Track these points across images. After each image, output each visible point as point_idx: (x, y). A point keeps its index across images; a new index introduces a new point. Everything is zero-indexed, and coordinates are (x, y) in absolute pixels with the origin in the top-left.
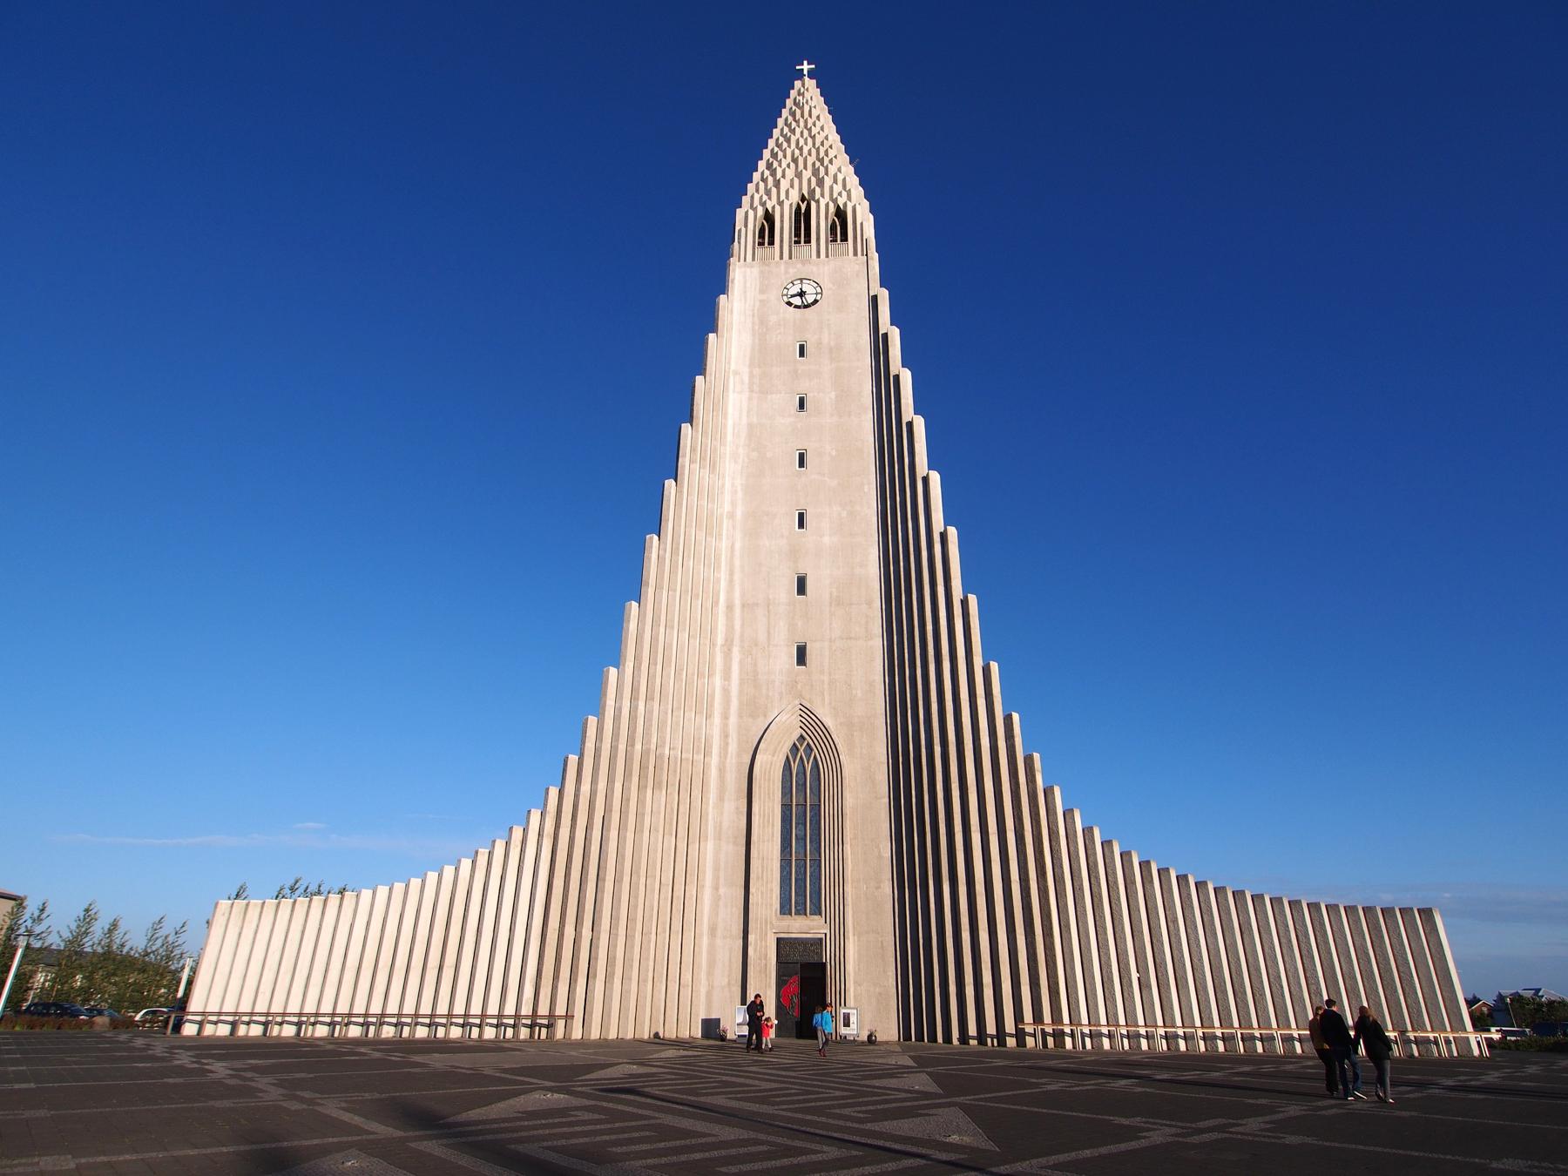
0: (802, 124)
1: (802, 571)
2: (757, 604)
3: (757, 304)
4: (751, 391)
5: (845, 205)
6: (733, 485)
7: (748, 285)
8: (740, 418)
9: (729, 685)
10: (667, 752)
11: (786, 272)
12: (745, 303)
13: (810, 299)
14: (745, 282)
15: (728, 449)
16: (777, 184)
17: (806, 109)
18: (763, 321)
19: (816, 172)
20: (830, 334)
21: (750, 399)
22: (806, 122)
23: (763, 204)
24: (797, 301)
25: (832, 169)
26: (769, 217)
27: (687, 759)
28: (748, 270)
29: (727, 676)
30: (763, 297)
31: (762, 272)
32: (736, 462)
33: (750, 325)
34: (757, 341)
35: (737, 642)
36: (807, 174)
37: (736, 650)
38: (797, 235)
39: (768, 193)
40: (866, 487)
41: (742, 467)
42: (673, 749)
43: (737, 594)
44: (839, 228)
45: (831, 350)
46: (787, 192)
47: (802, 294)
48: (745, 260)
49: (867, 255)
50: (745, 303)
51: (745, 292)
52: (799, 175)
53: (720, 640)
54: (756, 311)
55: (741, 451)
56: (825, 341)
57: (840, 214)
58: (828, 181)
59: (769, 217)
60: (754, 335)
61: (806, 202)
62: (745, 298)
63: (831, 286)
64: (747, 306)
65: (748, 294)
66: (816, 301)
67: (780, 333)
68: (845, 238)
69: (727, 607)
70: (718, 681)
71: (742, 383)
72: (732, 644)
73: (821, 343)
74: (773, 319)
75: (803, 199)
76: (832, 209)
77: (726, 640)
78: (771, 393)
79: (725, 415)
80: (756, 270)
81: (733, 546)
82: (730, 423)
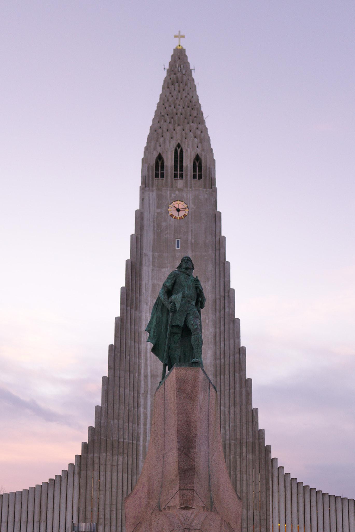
0: (177, 88)
2: (158, 375)
3: (156, 214)
4: (154, 266)
5: (202, 154)
6: (146, 316)
7: (151, 202)
8: (148, 281)
9: (146, 411)
10: (123, 441)
11: (171, 196)
12: (150, 214)
13: (182, 214)
14: (149, 201)
15: (143, 298)
18: (159, 226)
20: (192, 235)
21: (153, 270)
22: (179, 86)
24: (175, 213)
26: (160, 158)
27: (130, 443)
28: (151, 193)
29: (145, 408)
30: (159, 211)
31: (158, 195)
32: (147, 304)
33: (152, 227)
34: (156, 236)
35: (149, 392)
37: (149, 396)
38: (176, 169)
40: (207, 320)
41: (150, 306)
42: (125, 439)
43: (149, 370)
44: (197, 168)
45: (192, 244)
46: (170, 142)
48: (149, 187)
49: (211, 188)
50: (150, 214)
51: (149, 207)
53: (142, 392)
54: (155, 219)
55: (149, 298)
56: (190, 239)
57: (197, 158)
59: (160, 158)
60: (154, 234)
61: (180, 149)
62: (150, 212)
63: (193, 206)
64: (151, 215)
65: (151, 209)
66: (185, 216)
67: (167, 233)
68: (200, 177)
69: (145, 376)
70: (142, 409)
71: (149, 261)
72: (147, 393)
73: (187, 241)
74: (164, 224)
75: (179, 146)
77: (144, 391)
78: (164, 268)
79: (141, 279)
80: (155, 193)
81: (146, 347)
82: (144, 283)
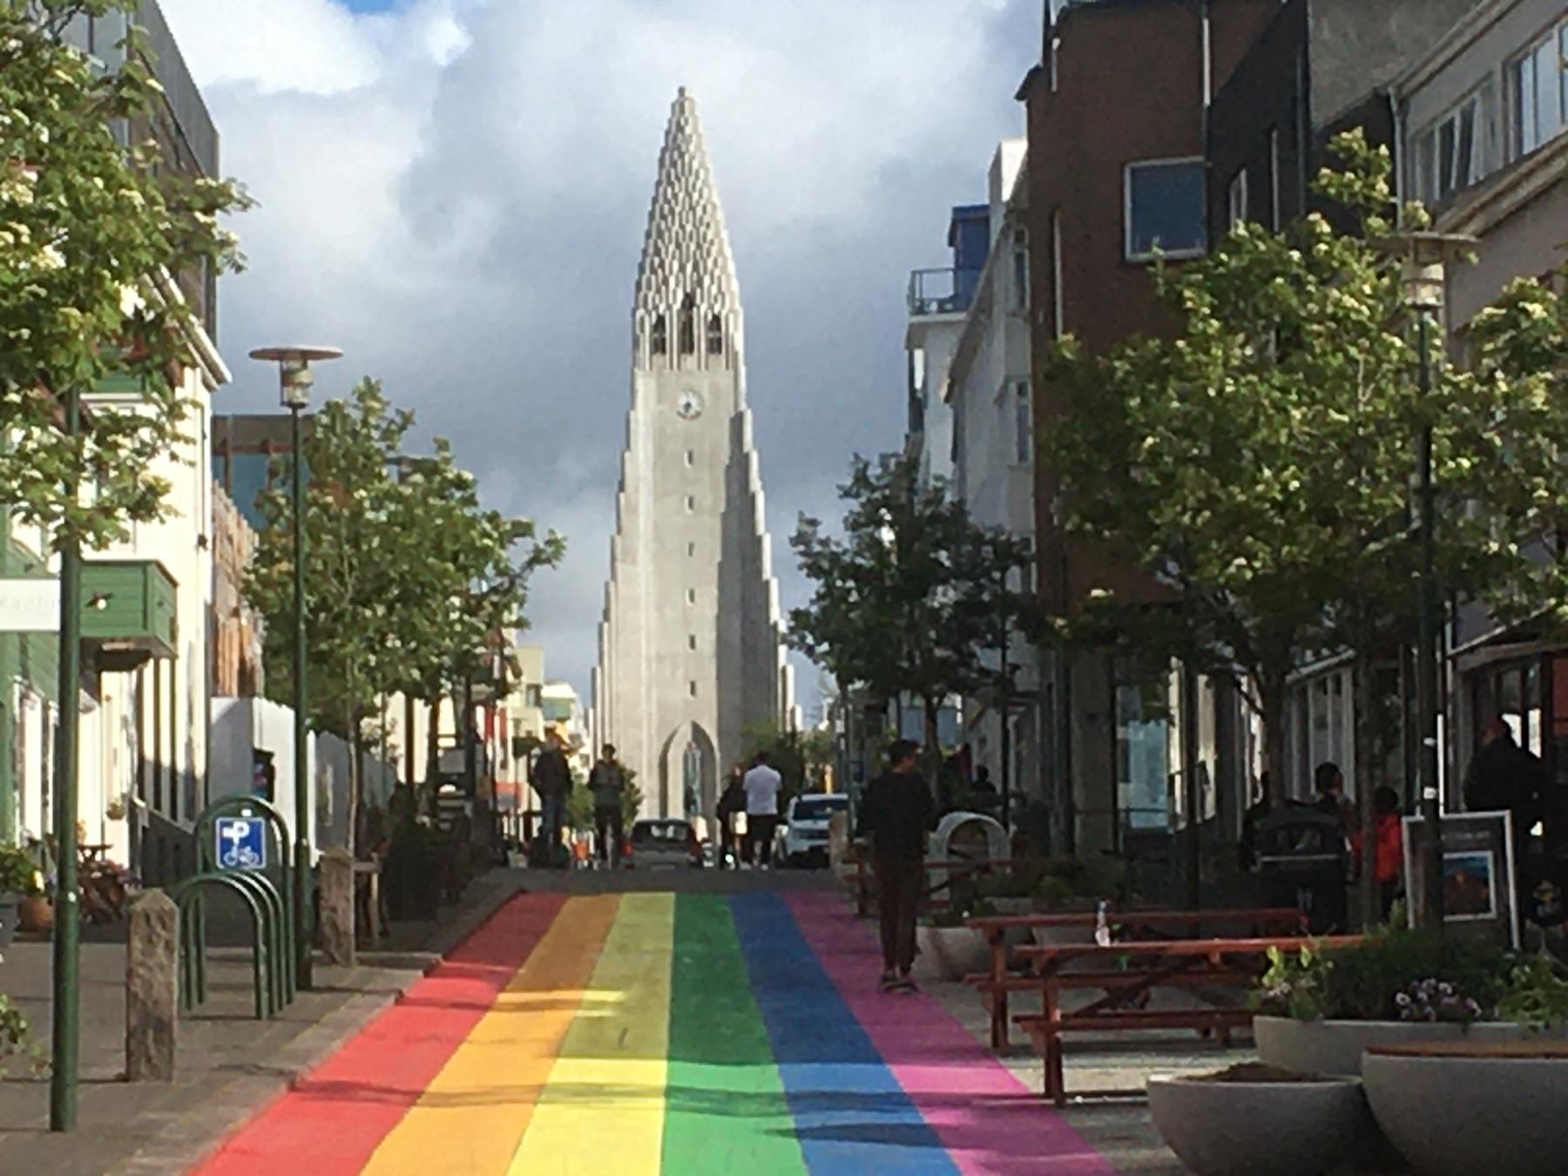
1: (692, 632)
13: (692, 412)
16: (666, 281)
17: (687, 158)
19: (696, 267)
23: (656, 308)
25: (710, 263)
26: (661, 320)
36: (689, 267)
39: (658, 291)
47: (688, 406)
52: (682, 268)
58: (707, 280)
59: (661, 320)
66: (698, 414)
70: (644, 705)
76: (710, 317)
